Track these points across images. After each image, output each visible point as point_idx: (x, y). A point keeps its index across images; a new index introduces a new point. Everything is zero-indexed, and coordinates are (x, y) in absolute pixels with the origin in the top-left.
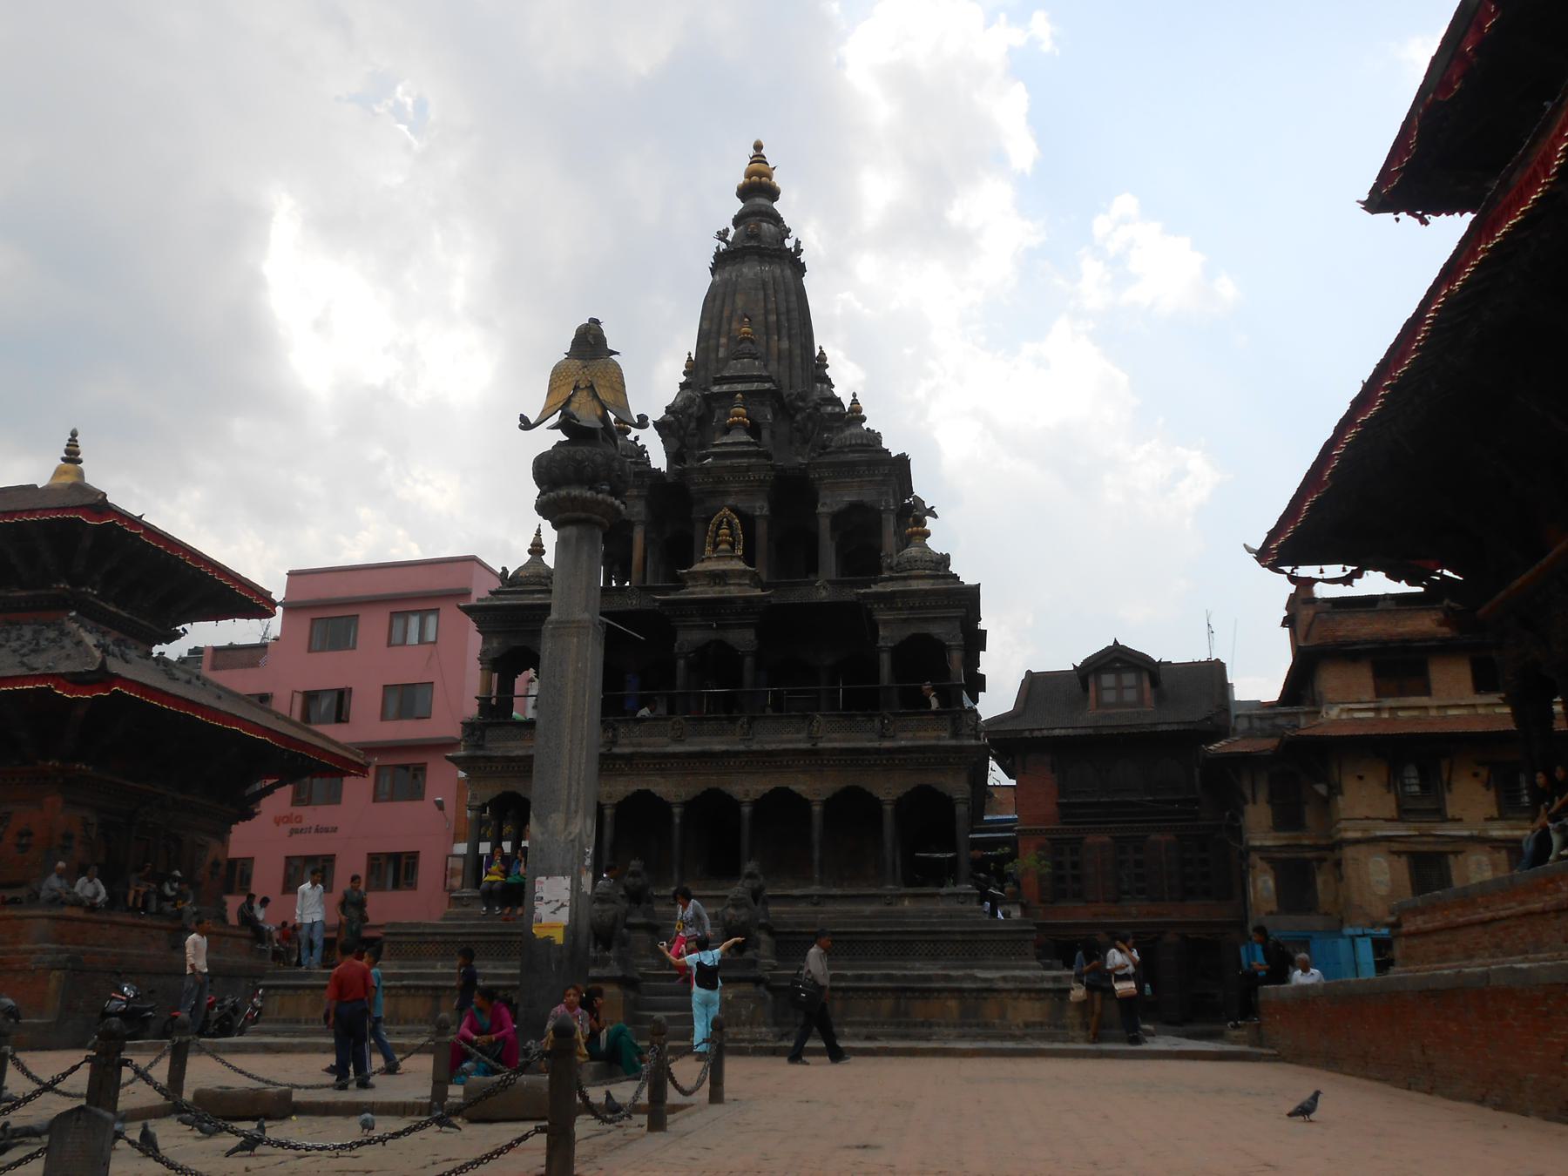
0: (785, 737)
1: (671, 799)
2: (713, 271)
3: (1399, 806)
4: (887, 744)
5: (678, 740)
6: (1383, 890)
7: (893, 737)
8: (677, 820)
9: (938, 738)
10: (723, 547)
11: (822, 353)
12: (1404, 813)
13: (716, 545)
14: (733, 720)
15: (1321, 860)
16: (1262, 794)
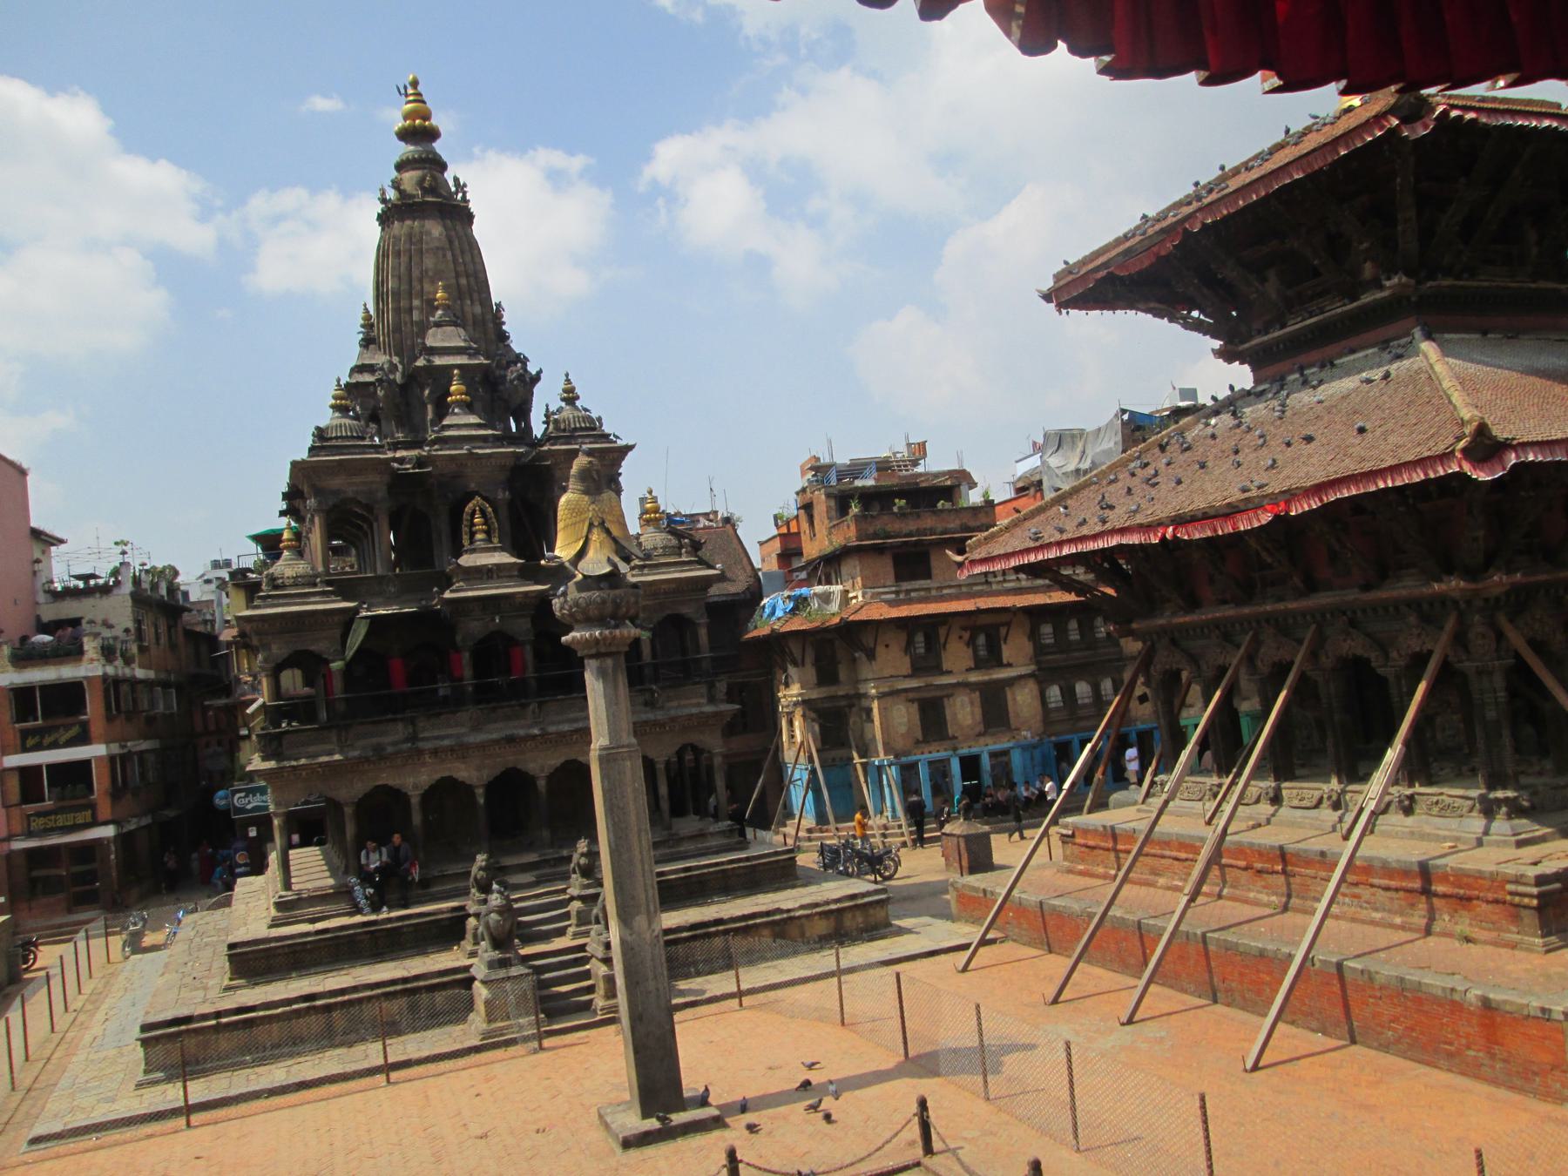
0: (572, 716)
1: (475, 782)
2: (384, 219)
3: (913, 665)
4: (659, 715)
5: (476, 728)
6: (903, 729)
7: (662, 708)
8: (482, 801)
9: (699, 705)
10: (479, 536)
11: (498, 310)
12: (917, 670)
13: (472, 534)
14: (524, 706)
15: (851, 706)
16: (809, 659)
